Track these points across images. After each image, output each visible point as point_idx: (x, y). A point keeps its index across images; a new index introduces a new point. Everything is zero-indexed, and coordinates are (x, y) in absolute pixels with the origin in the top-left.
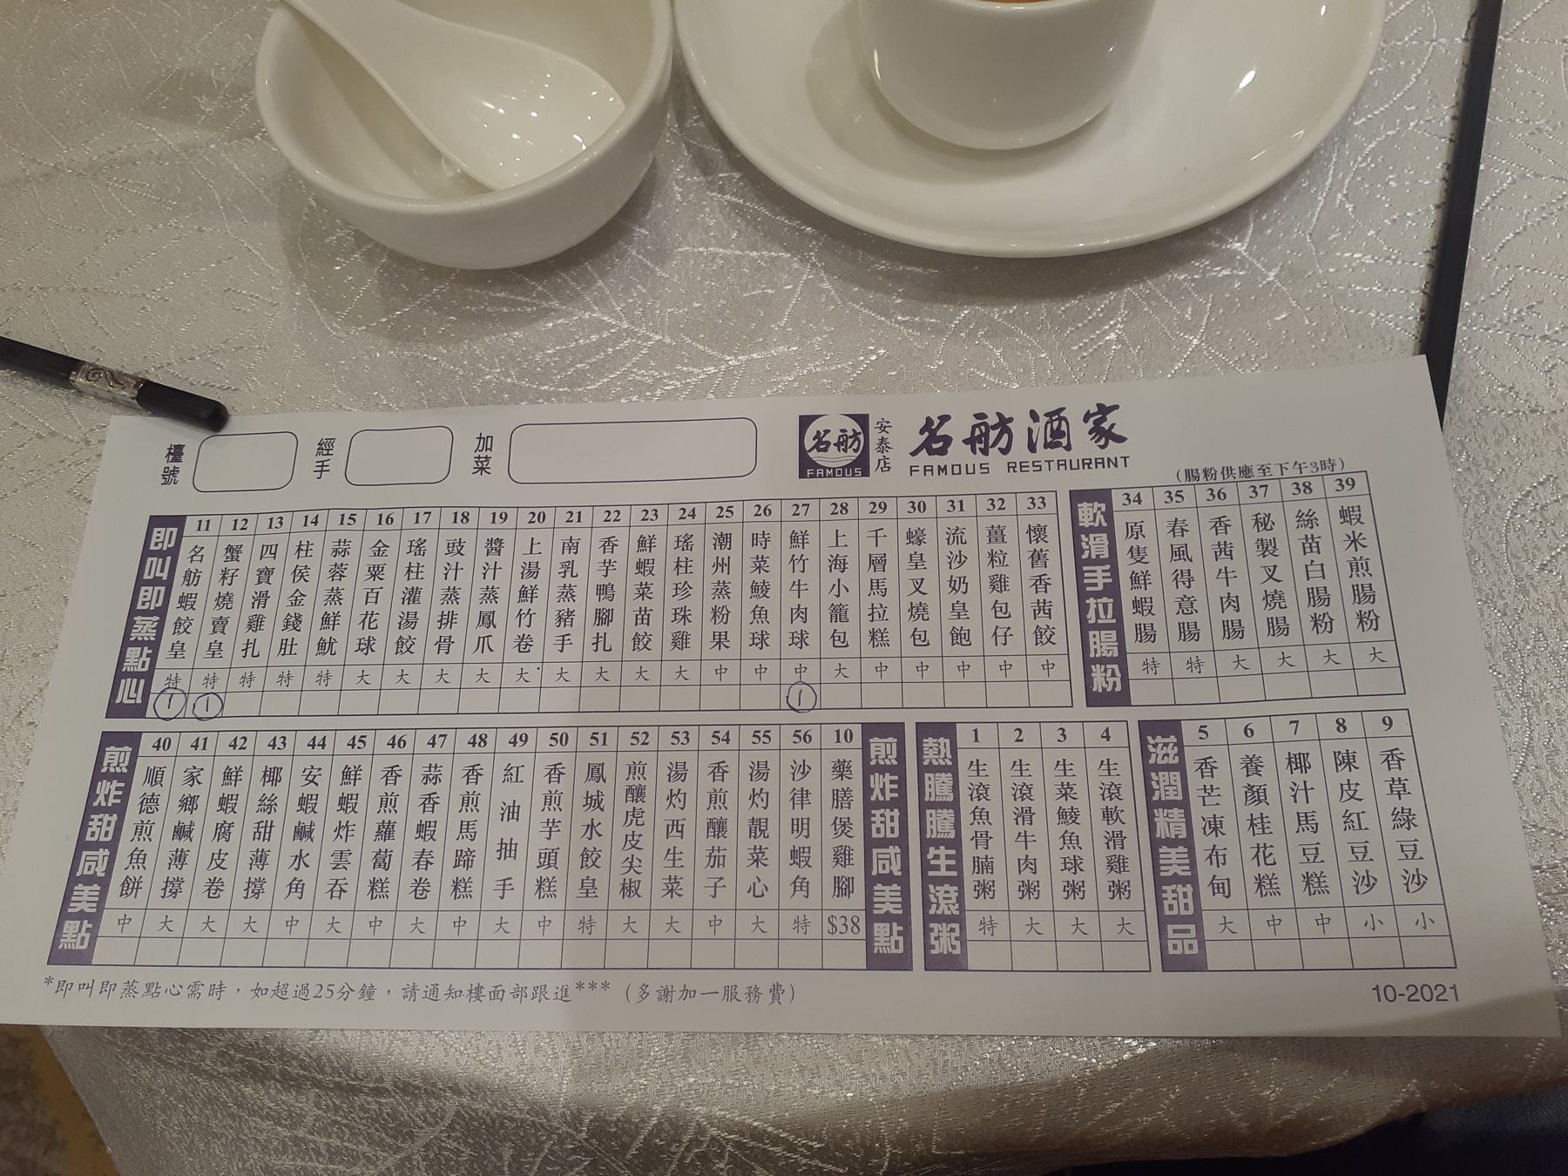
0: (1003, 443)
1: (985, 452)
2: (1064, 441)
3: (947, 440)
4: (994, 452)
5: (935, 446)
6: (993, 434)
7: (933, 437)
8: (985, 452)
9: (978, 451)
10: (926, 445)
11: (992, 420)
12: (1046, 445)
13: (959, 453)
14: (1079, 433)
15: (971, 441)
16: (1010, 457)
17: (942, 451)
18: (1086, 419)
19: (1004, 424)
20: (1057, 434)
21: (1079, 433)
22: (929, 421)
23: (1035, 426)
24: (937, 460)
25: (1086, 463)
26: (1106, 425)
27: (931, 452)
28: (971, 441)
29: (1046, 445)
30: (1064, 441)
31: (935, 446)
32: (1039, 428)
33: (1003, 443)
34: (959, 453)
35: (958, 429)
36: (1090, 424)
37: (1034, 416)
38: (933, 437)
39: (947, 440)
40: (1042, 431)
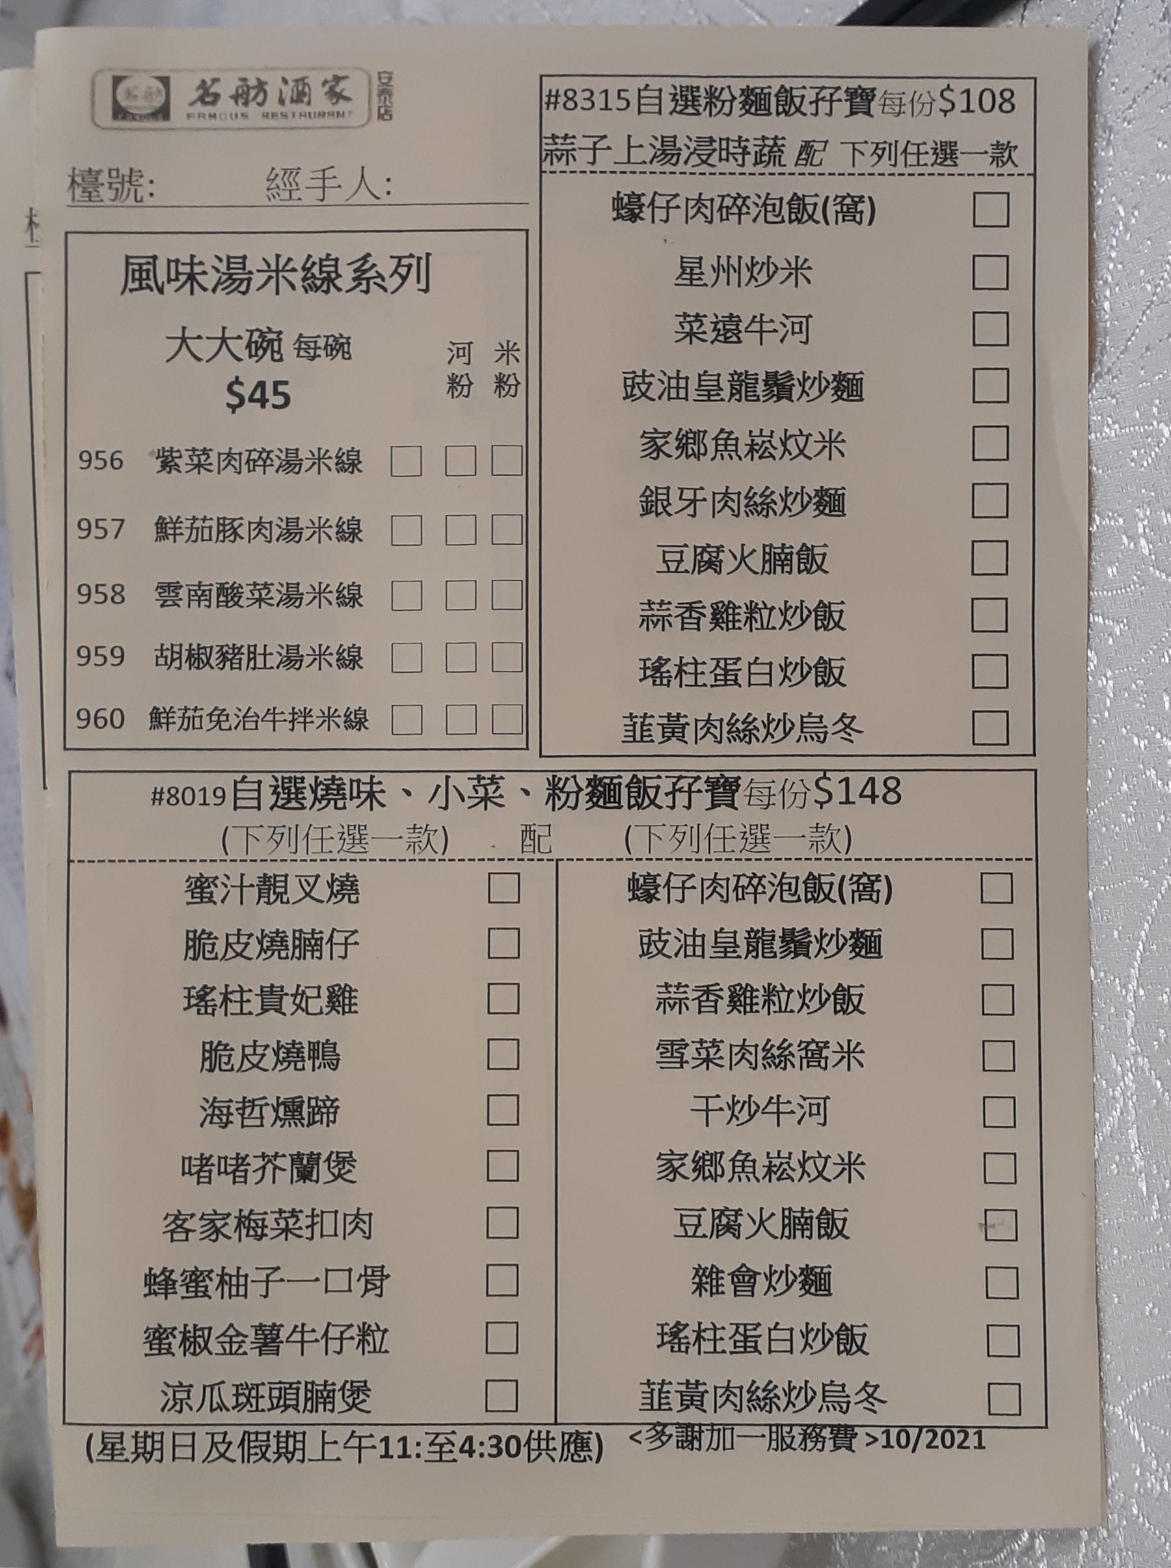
0: (260, 98)
1: (246, 104)
3: (217, 96)
4: (252, 105)
5: (207, 99)
6: (253, 93)
9: (240, 104)
12: (292, 101)
13: (226, 105)
15: (235, 98)
16: (266, 109)
23: (284, 88)
27: (204, 103)
28: (235, 98)
29: (292, 101)
33: (260, 98)
34: (226, 105)
35: (226, 88)
38: (206, 92)
39: (217, 96)
40: (290, 92)
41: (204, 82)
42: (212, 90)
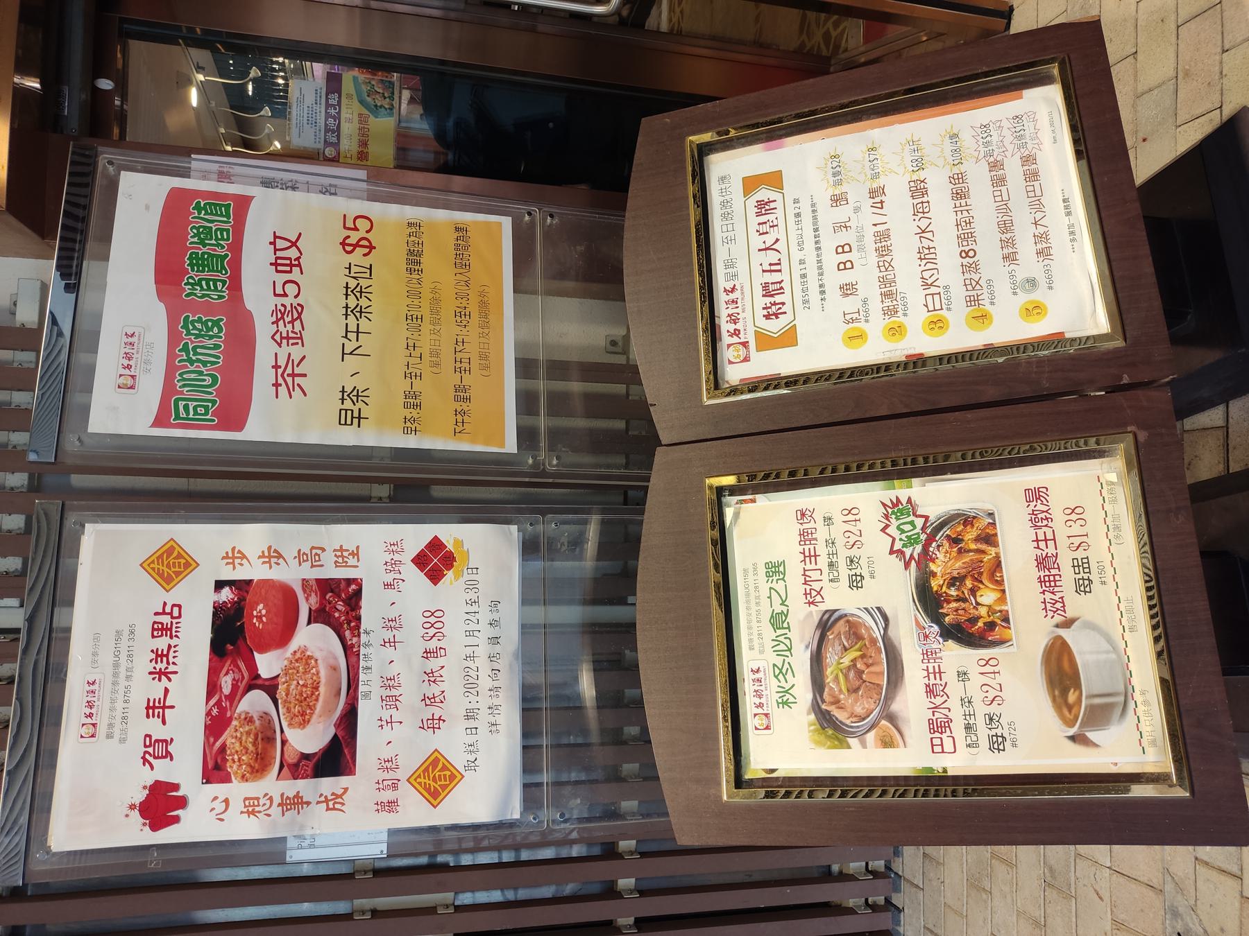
0: (736, 315)
1: (739, 319)
2: (735, 300)
4: (738, 317)
6: (733, 318)
7: (735, 334)
8: (739, 319)
10: (737, 335)
11: (729, 318)
13: (738, 326)
14: (732, 296)
17: (739, 331)
18: (728, 295)
19: (729, 315)
20: (733, 302)
21: (732, 296)
22: (729, 336)
24: (742, 332)
25: (742, 293)
26: (730, 290)
30: (735, 300)
31: (737, 332)
32: (730, 307)
33: (736, 315)
34: (738, 326)
36: (730, 294)
37: (728, 308)
39: (735, 330)
41: (729, 336)
42: (733, 332)
